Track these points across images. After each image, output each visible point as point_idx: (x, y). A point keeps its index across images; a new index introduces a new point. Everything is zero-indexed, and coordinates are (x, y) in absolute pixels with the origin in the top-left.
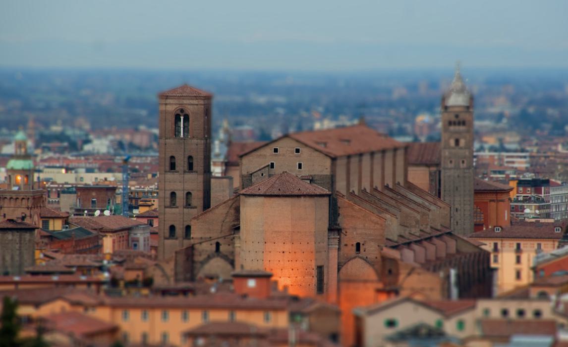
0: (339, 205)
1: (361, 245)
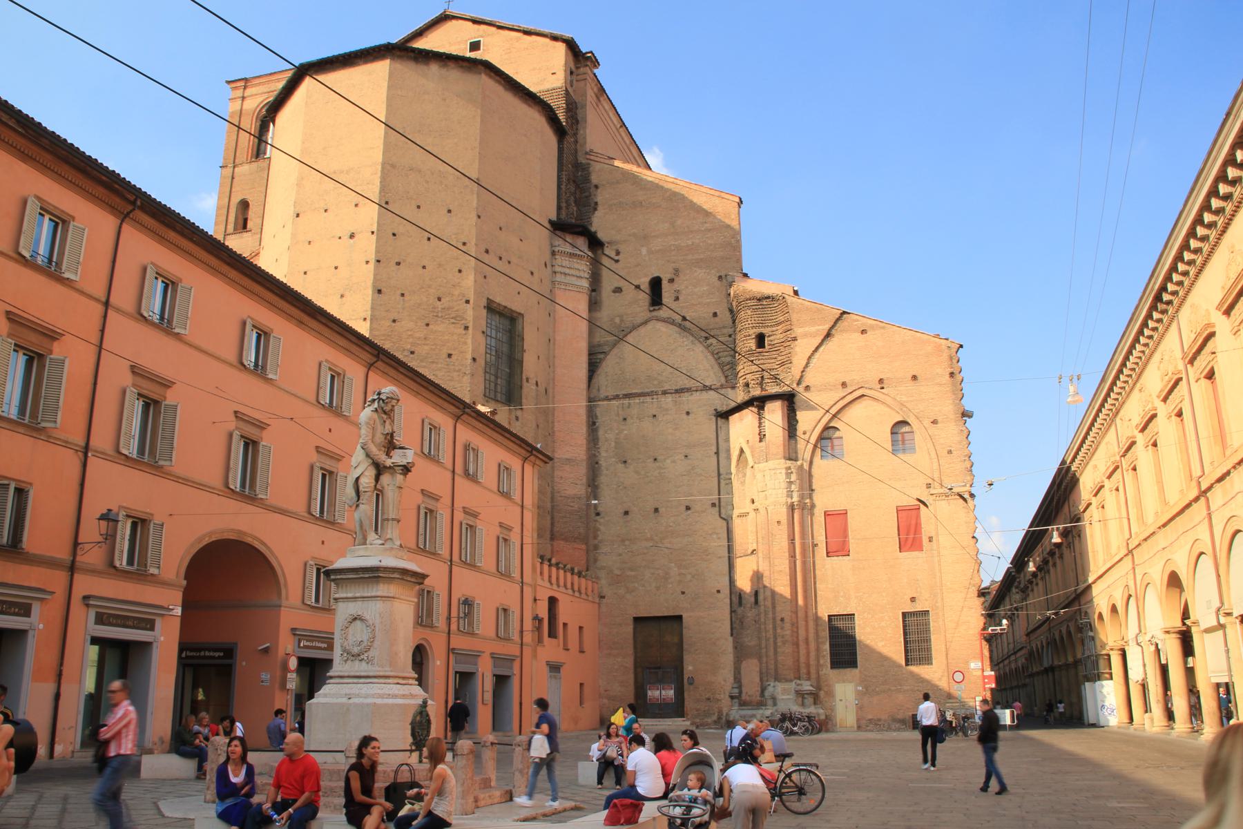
0: (594, 179)
1: (665, 284)
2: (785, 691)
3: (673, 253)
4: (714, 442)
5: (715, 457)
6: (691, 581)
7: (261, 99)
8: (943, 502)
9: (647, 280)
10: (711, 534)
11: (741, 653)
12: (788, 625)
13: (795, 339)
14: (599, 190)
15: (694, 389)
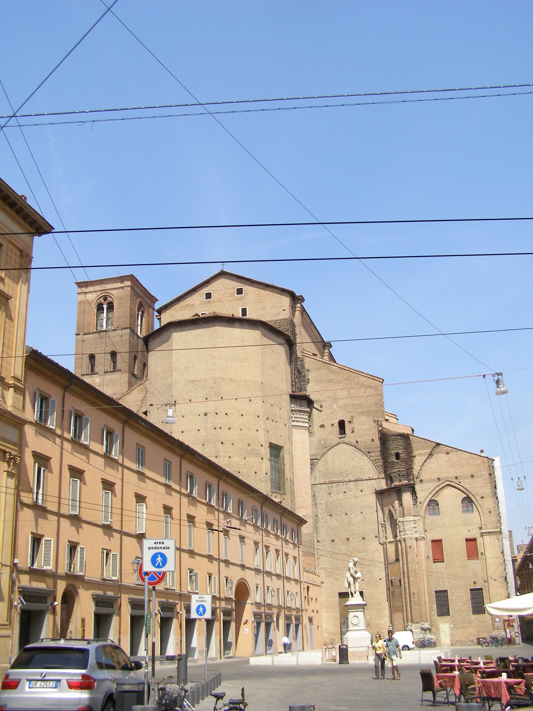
0: (307, 366)
1: (346, 424)
6: (366, 574)
7: (98, 294)
9: (337, 421)
10: (375, 551)
11: (393, 610)
13: (415, 457)
14: (310, 372)
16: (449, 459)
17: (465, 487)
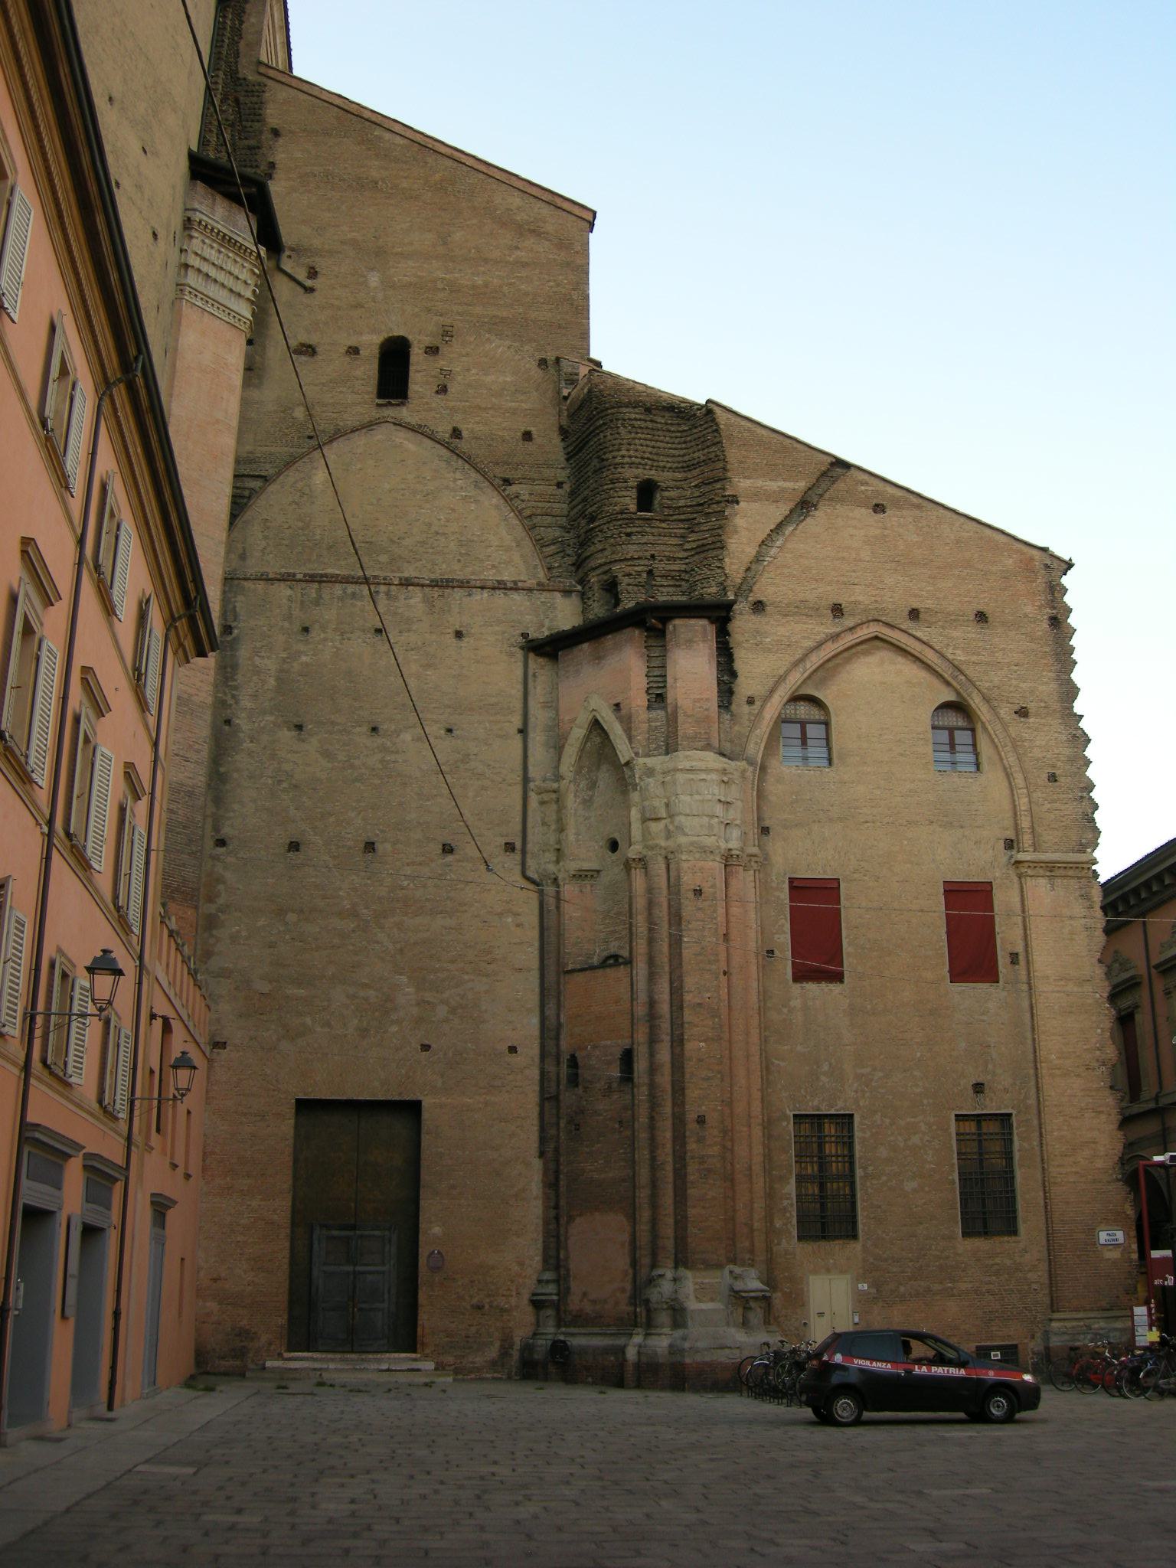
1: (417, 356)
2: (702, 1292)
3: (441, 295)
4: (518, 705)
5: (518, 740)
6: (447, 1020)
8: (1042, 881)
9: (377, 339)
10: (500, 914)
12: (716, 1132)
13: (734, 500)
14: (281, 141)
15: (478, 584)
16: (886, 532)
17: (951, 657)
